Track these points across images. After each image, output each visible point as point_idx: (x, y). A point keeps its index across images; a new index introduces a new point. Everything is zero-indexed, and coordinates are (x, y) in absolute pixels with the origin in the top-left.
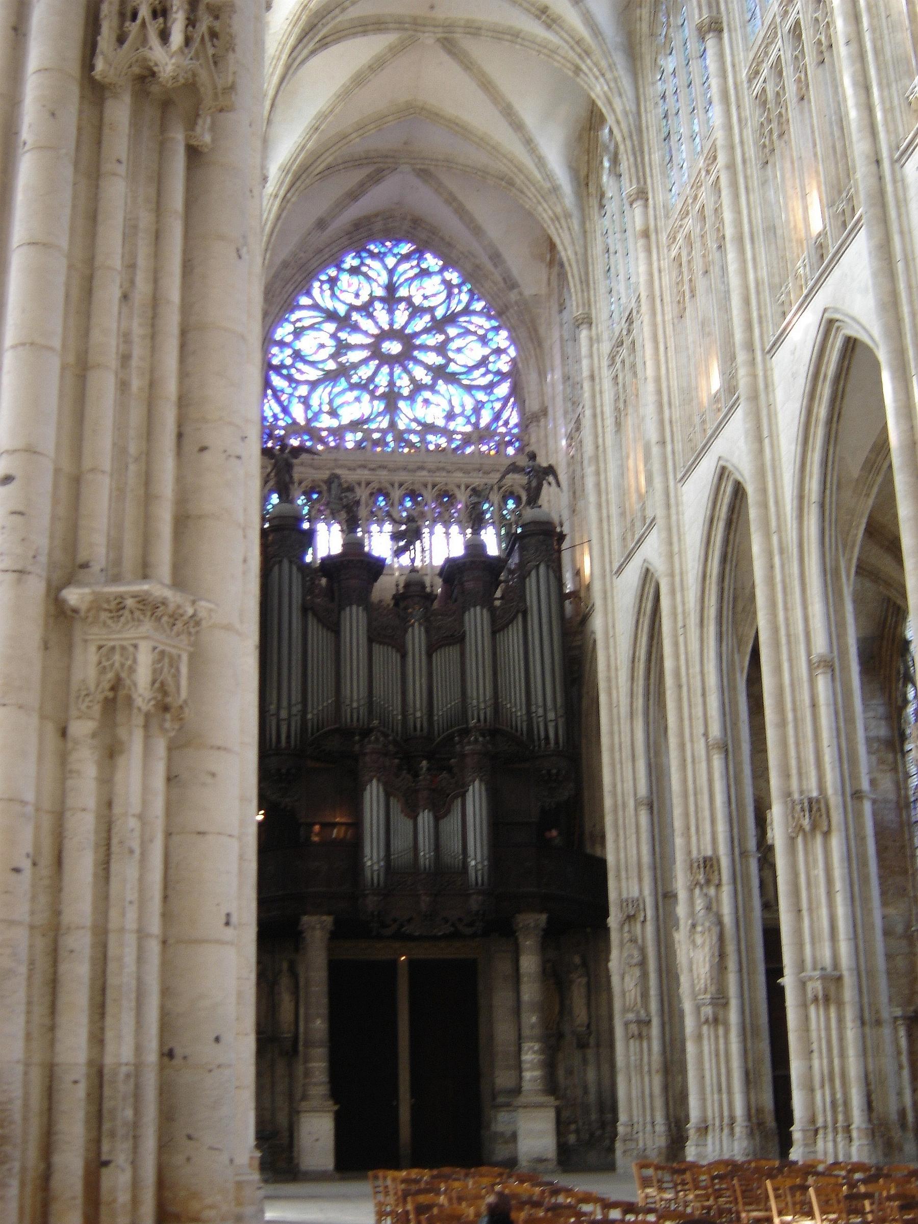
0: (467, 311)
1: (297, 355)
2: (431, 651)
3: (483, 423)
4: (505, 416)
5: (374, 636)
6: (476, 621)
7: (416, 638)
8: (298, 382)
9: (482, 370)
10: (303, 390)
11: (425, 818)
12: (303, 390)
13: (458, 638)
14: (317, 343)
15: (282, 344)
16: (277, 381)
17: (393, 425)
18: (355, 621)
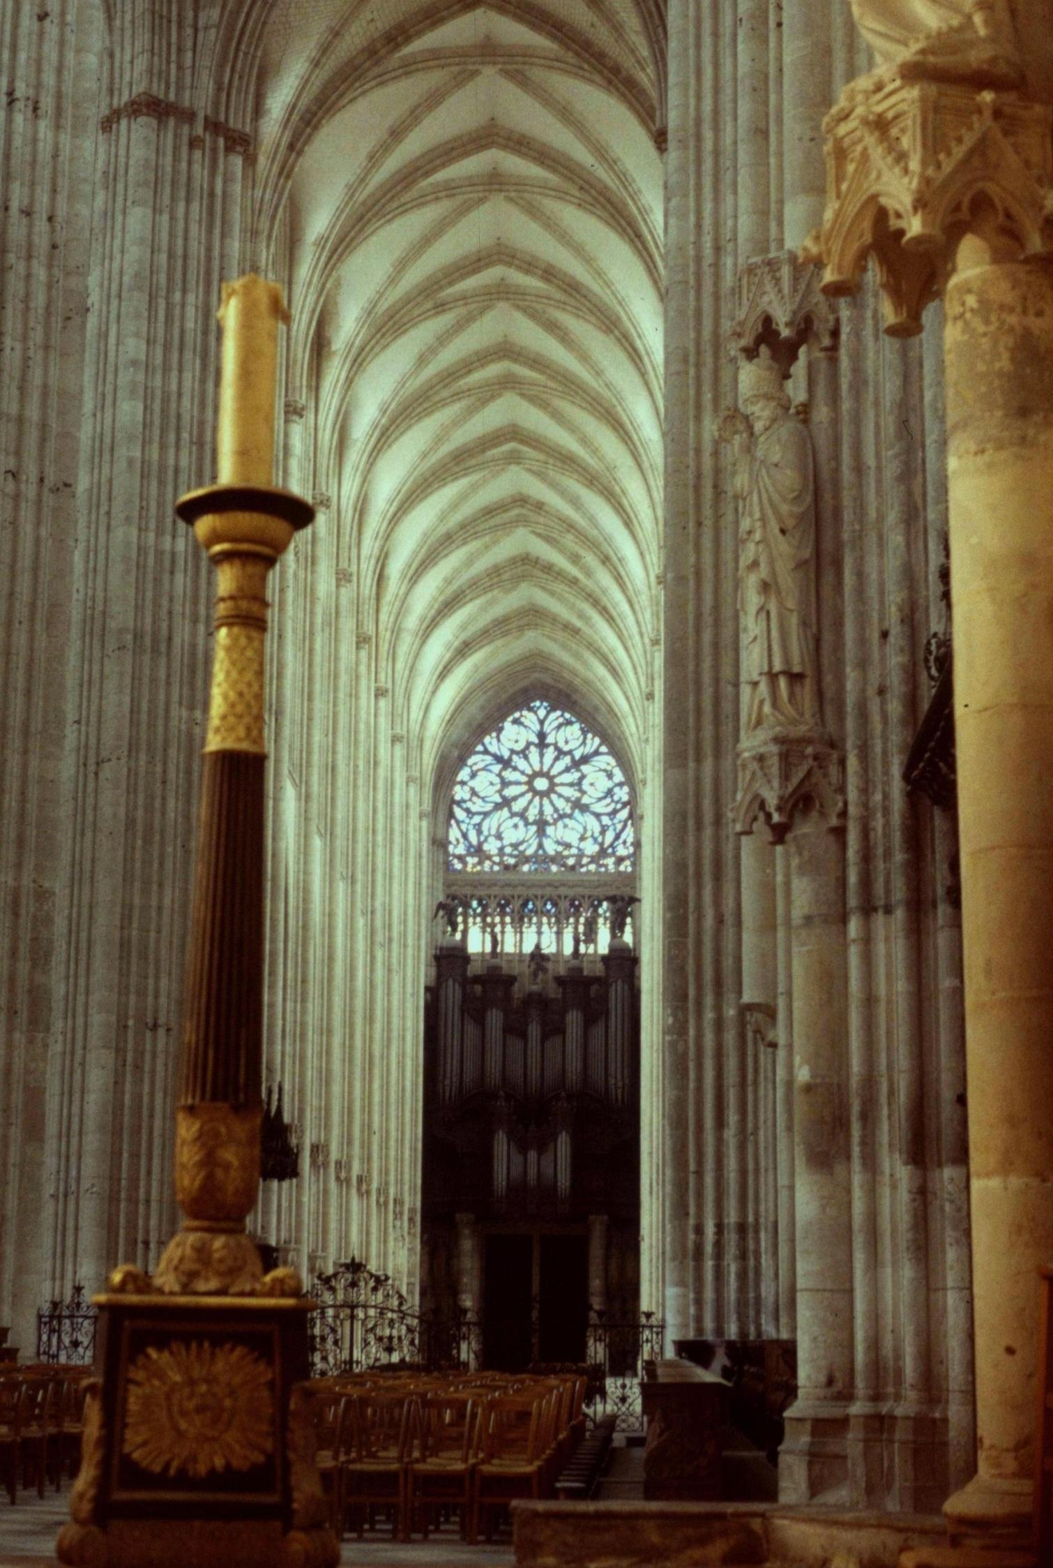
0: (597, 753)
1: (474, 793)
2: (545, 1037)
3: (607, 843)
4: (623, 836)
5: (507, 1030)
6: (574, 1019)
7: (534, 1031)
8: (474, 814)
9: (608, 800)
10: (477, 819)
11: (532, 1155)
12: (477, 819)
13: (561, 1030)
14: (486, 784)
15: (463, 783)
16: (459, 813)
17: (540, 846)
18: (495, 1019)
